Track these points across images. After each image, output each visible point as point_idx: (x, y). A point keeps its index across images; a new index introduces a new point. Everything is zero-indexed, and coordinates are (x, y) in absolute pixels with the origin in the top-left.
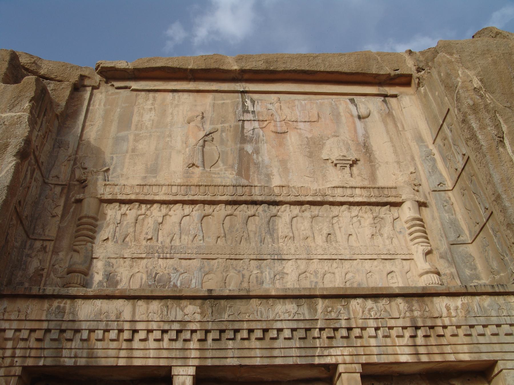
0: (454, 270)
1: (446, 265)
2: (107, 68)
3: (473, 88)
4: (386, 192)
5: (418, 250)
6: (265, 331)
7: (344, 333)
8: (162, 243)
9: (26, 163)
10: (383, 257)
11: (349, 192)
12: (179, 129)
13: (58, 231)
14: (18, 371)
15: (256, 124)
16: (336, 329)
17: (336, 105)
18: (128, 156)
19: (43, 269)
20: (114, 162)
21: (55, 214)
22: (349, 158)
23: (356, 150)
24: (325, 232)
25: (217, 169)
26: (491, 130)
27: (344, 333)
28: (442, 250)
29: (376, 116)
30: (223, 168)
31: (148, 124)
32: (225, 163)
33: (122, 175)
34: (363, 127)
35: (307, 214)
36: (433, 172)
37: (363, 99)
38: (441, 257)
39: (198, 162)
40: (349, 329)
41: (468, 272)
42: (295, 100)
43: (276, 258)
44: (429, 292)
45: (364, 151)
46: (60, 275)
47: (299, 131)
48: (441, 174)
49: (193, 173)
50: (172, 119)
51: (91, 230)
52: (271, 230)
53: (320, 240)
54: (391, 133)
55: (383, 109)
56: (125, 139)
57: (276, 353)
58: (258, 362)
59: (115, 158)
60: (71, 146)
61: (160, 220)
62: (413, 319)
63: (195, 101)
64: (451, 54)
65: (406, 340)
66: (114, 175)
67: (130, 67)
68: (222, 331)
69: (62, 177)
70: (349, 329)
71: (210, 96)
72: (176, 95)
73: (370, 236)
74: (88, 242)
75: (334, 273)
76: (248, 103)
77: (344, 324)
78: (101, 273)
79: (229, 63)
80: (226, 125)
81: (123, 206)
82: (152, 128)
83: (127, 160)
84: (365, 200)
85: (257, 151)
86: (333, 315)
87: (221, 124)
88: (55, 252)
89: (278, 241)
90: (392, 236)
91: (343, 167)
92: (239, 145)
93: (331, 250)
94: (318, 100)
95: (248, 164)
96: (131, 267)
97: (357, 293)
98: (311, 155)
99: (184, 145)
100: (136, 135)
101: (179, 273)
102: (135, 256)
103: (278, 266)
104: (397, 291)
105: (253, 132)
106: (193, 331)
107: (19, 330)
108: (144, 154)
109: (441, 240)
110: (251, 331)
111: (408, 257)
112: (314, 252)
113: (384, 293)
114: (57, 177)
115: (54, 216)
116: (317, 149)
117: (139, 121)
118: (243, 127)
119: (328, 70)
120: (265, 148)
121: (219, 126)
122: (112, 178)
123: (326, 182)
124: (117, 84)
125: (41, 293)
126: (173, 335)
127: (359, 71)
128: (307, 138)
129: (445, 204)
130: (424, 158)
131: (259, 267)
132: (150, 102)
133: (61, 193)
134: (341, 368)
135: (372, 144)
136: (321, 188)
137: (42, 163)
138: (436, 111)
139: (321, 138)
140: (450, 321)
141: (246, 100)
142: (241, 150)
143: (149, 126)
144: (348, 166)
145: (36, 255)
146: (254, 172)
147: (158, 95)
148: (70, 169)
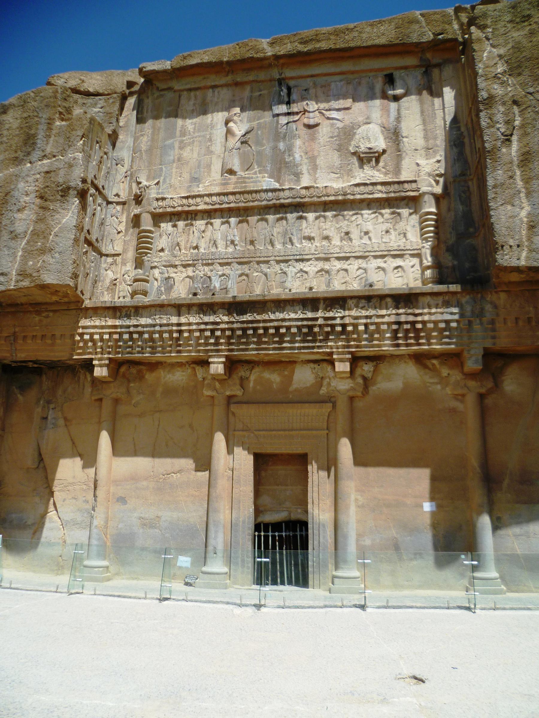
0: (456, 263)
1: (450, 258)
2: (148, 71)
3: (493, 75)
4: (406, 186)
6: (277, 328)
7: (339, 329)
8: (205, 249)
9: (89, 195)
10: (392, 253)
12: (219, 131)
13: (124, 245)
14: (107, 362)
16: (333, 326)
17: (373, 84)
18: (175, 165)
19: (116, 280)
20: (163, 175)
21: (120, 230)
22: (375, 151)
23: (385, 139)
24: (344, 231)
25: (251, 172)
27: (339, 329)
28: (451, 242)
30: (257, 170)
33: (171, 186)
34: (397, 108)
36: (458, 159)
37: (403, 73)
38: (448, 250)
39: (236, 168)
40: (344, 326)
41: (467, 265)
42: (332, 82)
43: (298, 257)
44: (414, 292)
45: (394, 138)
46: (129, 283)
47: (331, 121)
48: (466, 162)
49: (230, 179)
50: (212, 121)
51: (148, 243)
54: (425, 114)
55: (422, 83)
56: (172, 147)
57: (285, 345)
58: (271, 352)
59: (164, 169)
60: (126, 161)
61: (203, 228)
63: (234, 96)
64: (482, 28)
66: (165, 186)
67: (170, 68)
68: (244, 330)
69: (121, 194)
71: (248, 88)
72: (216, 91)
73: (383, 233)
74: (147, 254)
75: (346, 270)
77: (338, 321)
78: (159, 279)
79: (264, 49)
80: (262, 121)
81: (173, 217)
82: (194, 133)
83: (174, 170)
84: (384, 196)
85: (290, 149)
86: (331, 314)
87: (257, 120)
88: (124, 263)
89: (301, 241)
90: (405, 231)
91: (369, 161)
92: (272, 144)
93: (346, 249)
94: (355, 79)
95: (281, 164)
96: (182, 272)
97: (352, 295)
98: (340, 148)
99: (223, 149)
100: (181, 142)
101: (218, 276)
102: (184, 263)
103: (300, 266)
104: (387, 292)
105: (287, 127)
106: (223, 330)
107: (104, 333)
108: (189, 162)
109: (451, 233)
110: (266, 329)
111: (416, 252)
112: (332, 251)
113: (375, 294)
114: (117, 195)
115: (119, 233)
116: (346, 141)
117: (183, 125)
118: (278, 122)
119: (365, 45)
120: (298, 143)
121: (255, 124)
122: (162, 190)
123: (352, 177)
124: (162, 86)
125: (113, 305)
126: (208, 334)
127: (397, 41)
128: (338, 128)
129: (463, 195)
130: (452, 143)
132: (192, 103)
133: (123, 210)
134: (335, 356)
135: (403, 128)
136: (343, 186)
137: (103, 187)
138: (469, 91)
139: (353, 128)
140: (429, 317)
141: (283, 88)
143: (192, 130)
144: (374, 159)
145: (109, 268)
146: (285, 174)
147: (198, 93)
148: (128, 185)
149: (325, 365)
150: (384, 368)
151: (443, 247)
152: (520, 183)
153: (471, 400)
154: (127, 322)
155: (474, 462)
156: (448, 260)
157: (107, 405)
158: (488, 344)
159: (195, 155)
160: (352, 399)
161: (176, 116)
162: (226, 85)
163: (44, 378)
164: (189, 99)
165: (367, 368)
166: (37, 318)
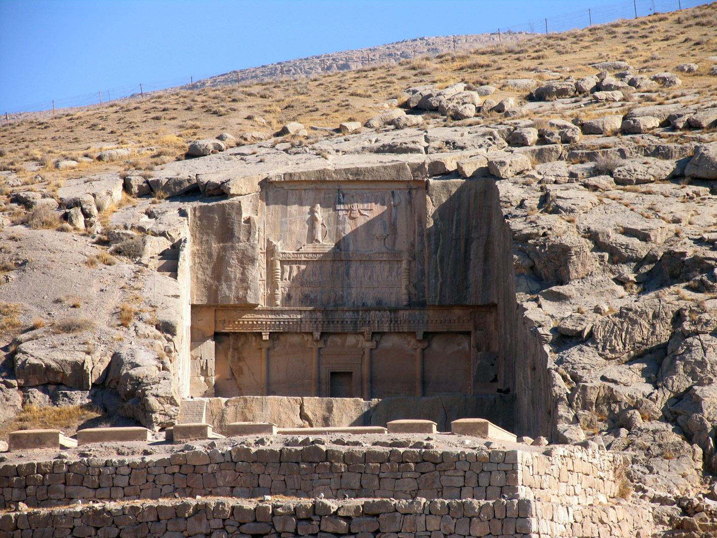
5: (404, 282)
11: (381, 255)
15: (344, 212)
24: (369, 274)
26: (433, 247)
29: (403, 203)
31: (294, 213)
32: (330, 237)
35: (363, 265)
41: (421, 294)
48: (424, 244)
52: (348, 274)
53: (367, 278)
62: (391, 319)
65: (387, 325)
70: (369, 322)
76: (341, 197)
131: (342, 291)
132: (294, 197)
142: (337, 228)
149: (360, 335)
150: (384, 337)
151: (412, 285)
152: (439, 270)
153: (419, 351)
154: (278, 317)
155: (419, 376)
156: (413, 291)
157: (264, 351)
158: (425, 330)
159: (298, 228)
160: (371, 350)
161: (287, 205)
162: (312, 189)
163: (231, 337)
164: (293, 195)
165: (377, 338)
166: (235, 313)
